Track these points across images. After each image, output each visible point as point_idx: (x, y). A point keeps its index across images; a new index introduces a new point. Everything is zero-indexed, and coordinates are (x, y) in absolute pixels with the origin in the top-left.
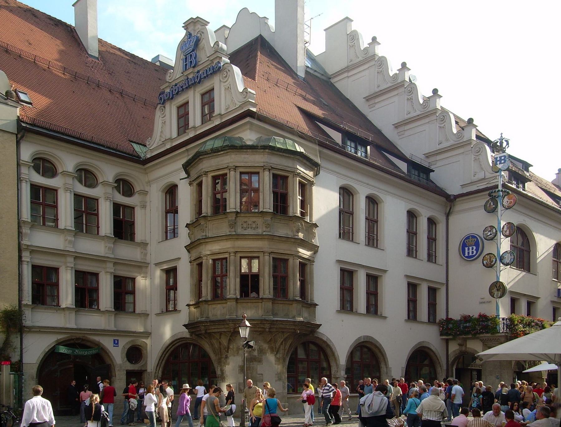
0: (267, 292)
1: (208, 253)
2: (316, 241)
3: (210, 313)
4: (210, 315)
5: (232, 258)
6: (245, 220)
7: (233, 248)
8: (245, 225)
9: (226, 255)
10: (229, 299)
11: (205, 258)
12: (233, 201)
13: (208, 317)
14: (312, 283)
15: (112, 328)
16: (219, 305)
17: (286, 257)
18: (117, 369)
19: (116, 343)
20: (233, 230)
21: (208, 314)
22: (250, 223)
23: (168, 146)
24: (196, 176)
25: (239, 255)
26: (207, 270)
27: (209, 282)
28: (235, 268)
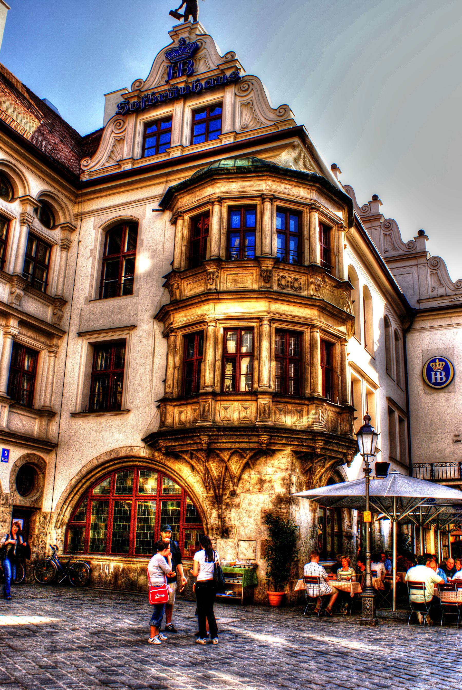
1: (221, 316)
3: (218, 415)
4: (218, 419)
5: (266, 328)
7: (269, 312)
9: (254, 324)
10: (264, 393)
11: (214, 324)
13: (214, 422)
16: (236, 404)
20: (268, 285)
21: (214, 418)
22: (289, 279)
23: (128, 167)
24: (196, 204)
25: (274, 325)
26: (215, 343)
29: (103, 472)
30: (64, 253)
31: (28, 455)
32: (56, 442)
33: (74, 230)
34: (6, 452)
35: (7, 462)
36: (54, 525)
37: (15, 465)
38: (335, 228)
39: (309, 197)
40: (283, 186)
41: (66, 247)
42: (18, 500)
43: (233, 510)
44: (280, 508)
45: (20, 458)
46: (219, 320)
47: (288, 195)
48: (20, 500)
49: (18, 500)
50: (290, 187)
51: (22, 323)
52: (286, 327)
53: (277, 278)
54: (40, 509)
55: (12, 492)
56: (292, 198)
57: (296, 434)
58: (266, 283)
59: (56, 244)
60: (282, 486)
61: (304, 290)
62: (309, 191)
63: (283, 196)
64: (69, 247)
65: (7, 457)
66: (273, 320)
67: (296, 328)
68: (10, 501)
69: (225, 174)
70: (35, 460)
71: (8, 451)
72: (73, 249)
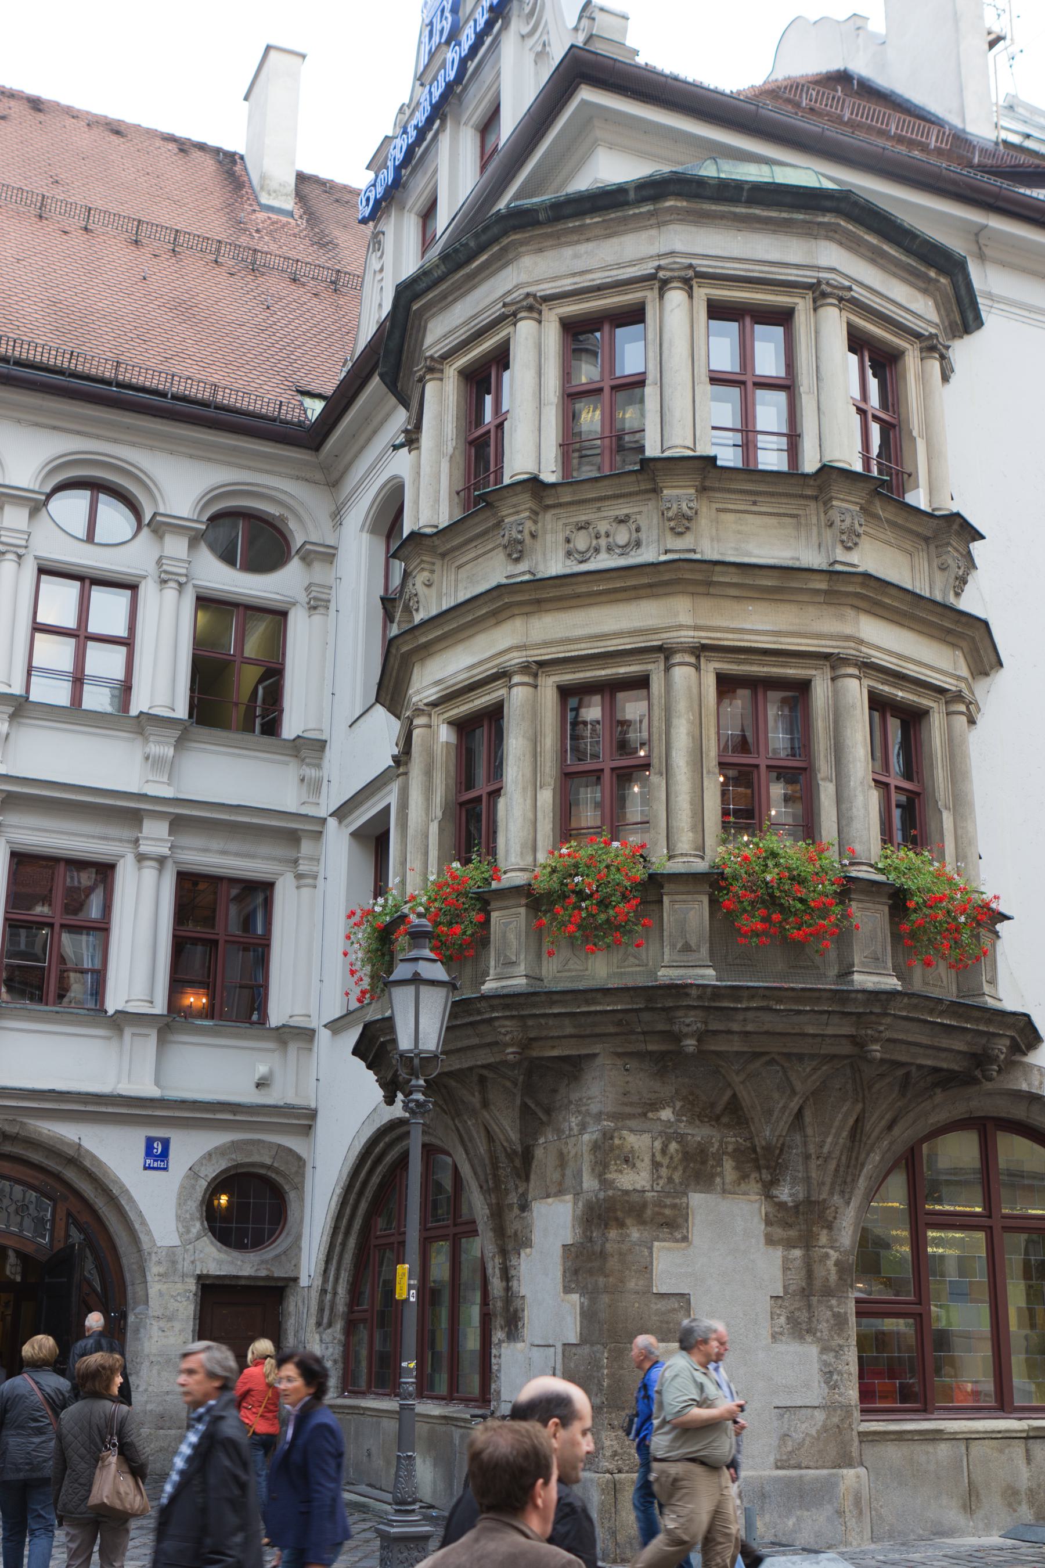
0: (685, 842)
2: (969, 603)
6: (584, 518)
8: (581, 542)
12: (531, 447)
14: (960, 804)
15: (148, 1089)
17: (791, 672)
18: (154, 1270)
19: (157, 1155)
22: (603, 527)
25: (549, 684)
26: (429, 773)
27: (434, 828)
28: (535, 741)
29: (380, 1169)
30: (317, 618)
31: (235, 1145)
32: (313, 1106)
33: (334, 555)
34: (158, 1148)
35: (165, 1169)
36: (313, 1321)
37: (193, 1172)
38: (802, 306)
39: (654, 250)
40: (568, 252)
41: (318, 604)
42: (217, 1260)
43: (523, 1255)
44: (590, 1240)
45: (209, 1155)
46: (434, 704)
47: (582, 273)
48: (220, 1262)
49: (217, 1260)
50: (590, 246)
51: (178, 824)
52: (588, 674)
53: (561, 538)
54: (296, 1280)
55: (185, 1243)
56: (598, 278)
57: (588, 1003)
58: (517, 560)
59: (294, 604)
60: (593, 1170)
61: (648, 545)
62: (653, 232)
63: (567, 284)
64: (329, 601)
65: (165, 1155)
66: (541, 664)
67: (622, 670)
68: (186, 1266)
69: (429, 289)
70: (256, 1158)
71: (166, 1143)
72: (333, 606)
